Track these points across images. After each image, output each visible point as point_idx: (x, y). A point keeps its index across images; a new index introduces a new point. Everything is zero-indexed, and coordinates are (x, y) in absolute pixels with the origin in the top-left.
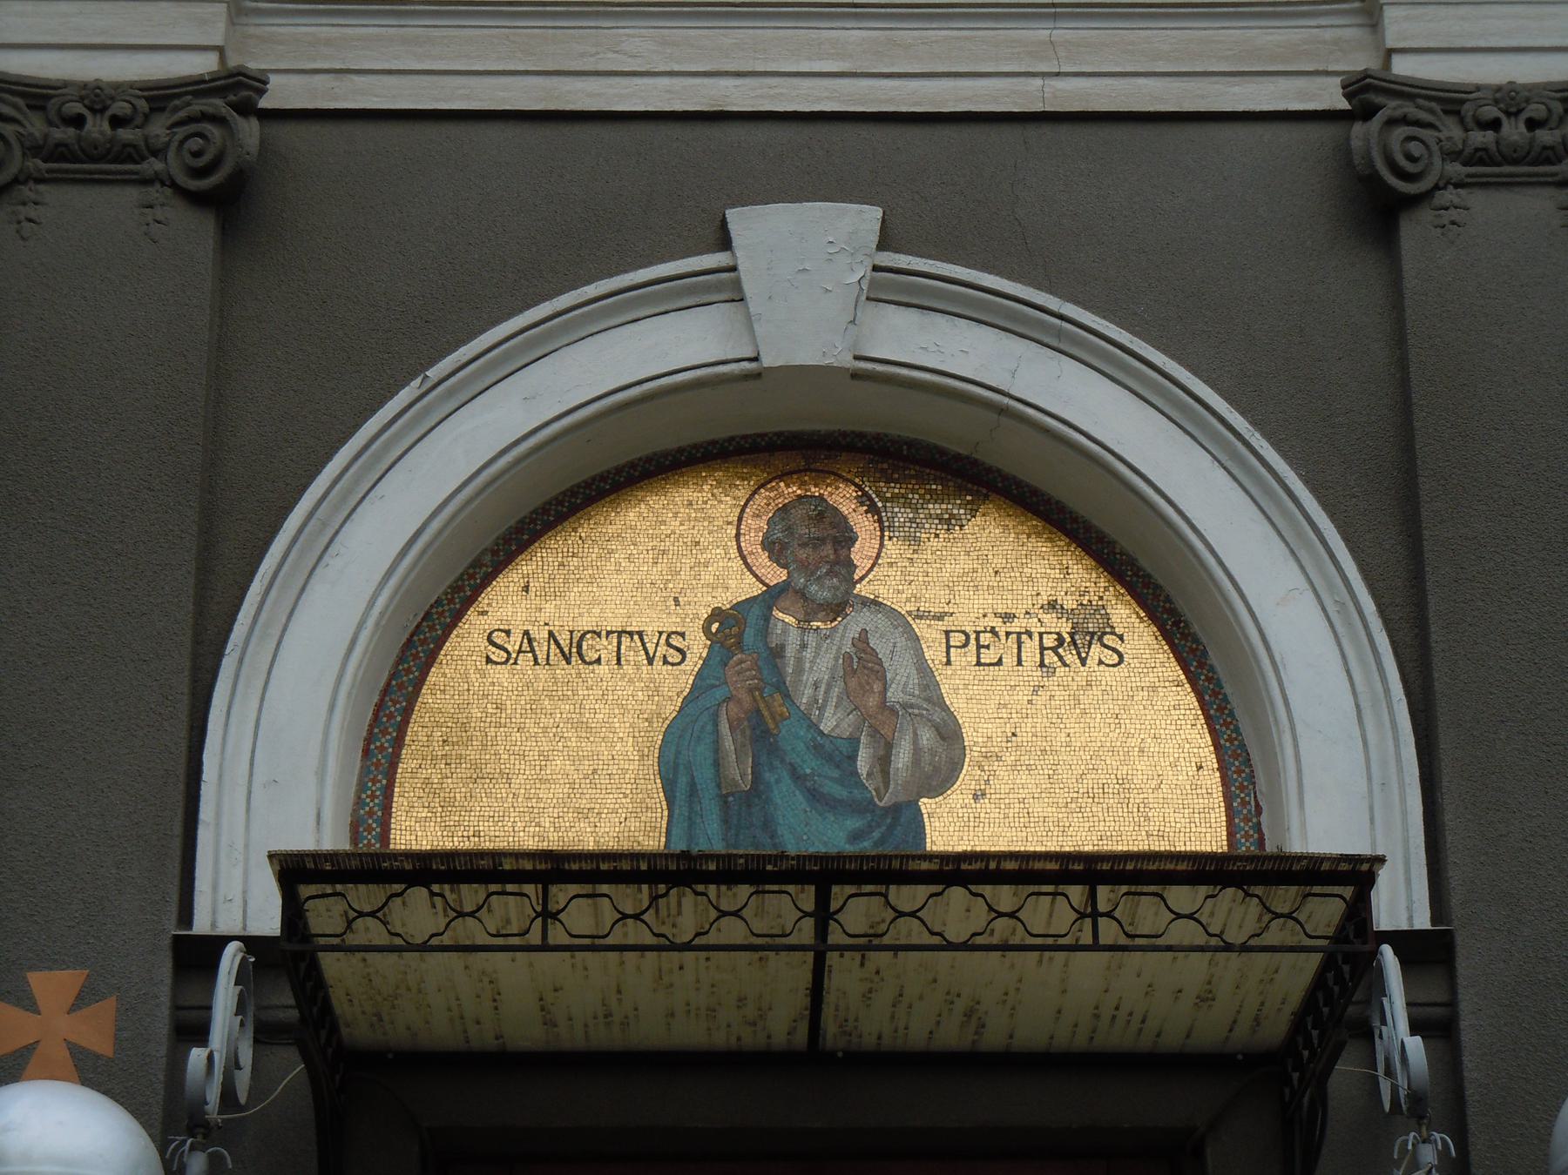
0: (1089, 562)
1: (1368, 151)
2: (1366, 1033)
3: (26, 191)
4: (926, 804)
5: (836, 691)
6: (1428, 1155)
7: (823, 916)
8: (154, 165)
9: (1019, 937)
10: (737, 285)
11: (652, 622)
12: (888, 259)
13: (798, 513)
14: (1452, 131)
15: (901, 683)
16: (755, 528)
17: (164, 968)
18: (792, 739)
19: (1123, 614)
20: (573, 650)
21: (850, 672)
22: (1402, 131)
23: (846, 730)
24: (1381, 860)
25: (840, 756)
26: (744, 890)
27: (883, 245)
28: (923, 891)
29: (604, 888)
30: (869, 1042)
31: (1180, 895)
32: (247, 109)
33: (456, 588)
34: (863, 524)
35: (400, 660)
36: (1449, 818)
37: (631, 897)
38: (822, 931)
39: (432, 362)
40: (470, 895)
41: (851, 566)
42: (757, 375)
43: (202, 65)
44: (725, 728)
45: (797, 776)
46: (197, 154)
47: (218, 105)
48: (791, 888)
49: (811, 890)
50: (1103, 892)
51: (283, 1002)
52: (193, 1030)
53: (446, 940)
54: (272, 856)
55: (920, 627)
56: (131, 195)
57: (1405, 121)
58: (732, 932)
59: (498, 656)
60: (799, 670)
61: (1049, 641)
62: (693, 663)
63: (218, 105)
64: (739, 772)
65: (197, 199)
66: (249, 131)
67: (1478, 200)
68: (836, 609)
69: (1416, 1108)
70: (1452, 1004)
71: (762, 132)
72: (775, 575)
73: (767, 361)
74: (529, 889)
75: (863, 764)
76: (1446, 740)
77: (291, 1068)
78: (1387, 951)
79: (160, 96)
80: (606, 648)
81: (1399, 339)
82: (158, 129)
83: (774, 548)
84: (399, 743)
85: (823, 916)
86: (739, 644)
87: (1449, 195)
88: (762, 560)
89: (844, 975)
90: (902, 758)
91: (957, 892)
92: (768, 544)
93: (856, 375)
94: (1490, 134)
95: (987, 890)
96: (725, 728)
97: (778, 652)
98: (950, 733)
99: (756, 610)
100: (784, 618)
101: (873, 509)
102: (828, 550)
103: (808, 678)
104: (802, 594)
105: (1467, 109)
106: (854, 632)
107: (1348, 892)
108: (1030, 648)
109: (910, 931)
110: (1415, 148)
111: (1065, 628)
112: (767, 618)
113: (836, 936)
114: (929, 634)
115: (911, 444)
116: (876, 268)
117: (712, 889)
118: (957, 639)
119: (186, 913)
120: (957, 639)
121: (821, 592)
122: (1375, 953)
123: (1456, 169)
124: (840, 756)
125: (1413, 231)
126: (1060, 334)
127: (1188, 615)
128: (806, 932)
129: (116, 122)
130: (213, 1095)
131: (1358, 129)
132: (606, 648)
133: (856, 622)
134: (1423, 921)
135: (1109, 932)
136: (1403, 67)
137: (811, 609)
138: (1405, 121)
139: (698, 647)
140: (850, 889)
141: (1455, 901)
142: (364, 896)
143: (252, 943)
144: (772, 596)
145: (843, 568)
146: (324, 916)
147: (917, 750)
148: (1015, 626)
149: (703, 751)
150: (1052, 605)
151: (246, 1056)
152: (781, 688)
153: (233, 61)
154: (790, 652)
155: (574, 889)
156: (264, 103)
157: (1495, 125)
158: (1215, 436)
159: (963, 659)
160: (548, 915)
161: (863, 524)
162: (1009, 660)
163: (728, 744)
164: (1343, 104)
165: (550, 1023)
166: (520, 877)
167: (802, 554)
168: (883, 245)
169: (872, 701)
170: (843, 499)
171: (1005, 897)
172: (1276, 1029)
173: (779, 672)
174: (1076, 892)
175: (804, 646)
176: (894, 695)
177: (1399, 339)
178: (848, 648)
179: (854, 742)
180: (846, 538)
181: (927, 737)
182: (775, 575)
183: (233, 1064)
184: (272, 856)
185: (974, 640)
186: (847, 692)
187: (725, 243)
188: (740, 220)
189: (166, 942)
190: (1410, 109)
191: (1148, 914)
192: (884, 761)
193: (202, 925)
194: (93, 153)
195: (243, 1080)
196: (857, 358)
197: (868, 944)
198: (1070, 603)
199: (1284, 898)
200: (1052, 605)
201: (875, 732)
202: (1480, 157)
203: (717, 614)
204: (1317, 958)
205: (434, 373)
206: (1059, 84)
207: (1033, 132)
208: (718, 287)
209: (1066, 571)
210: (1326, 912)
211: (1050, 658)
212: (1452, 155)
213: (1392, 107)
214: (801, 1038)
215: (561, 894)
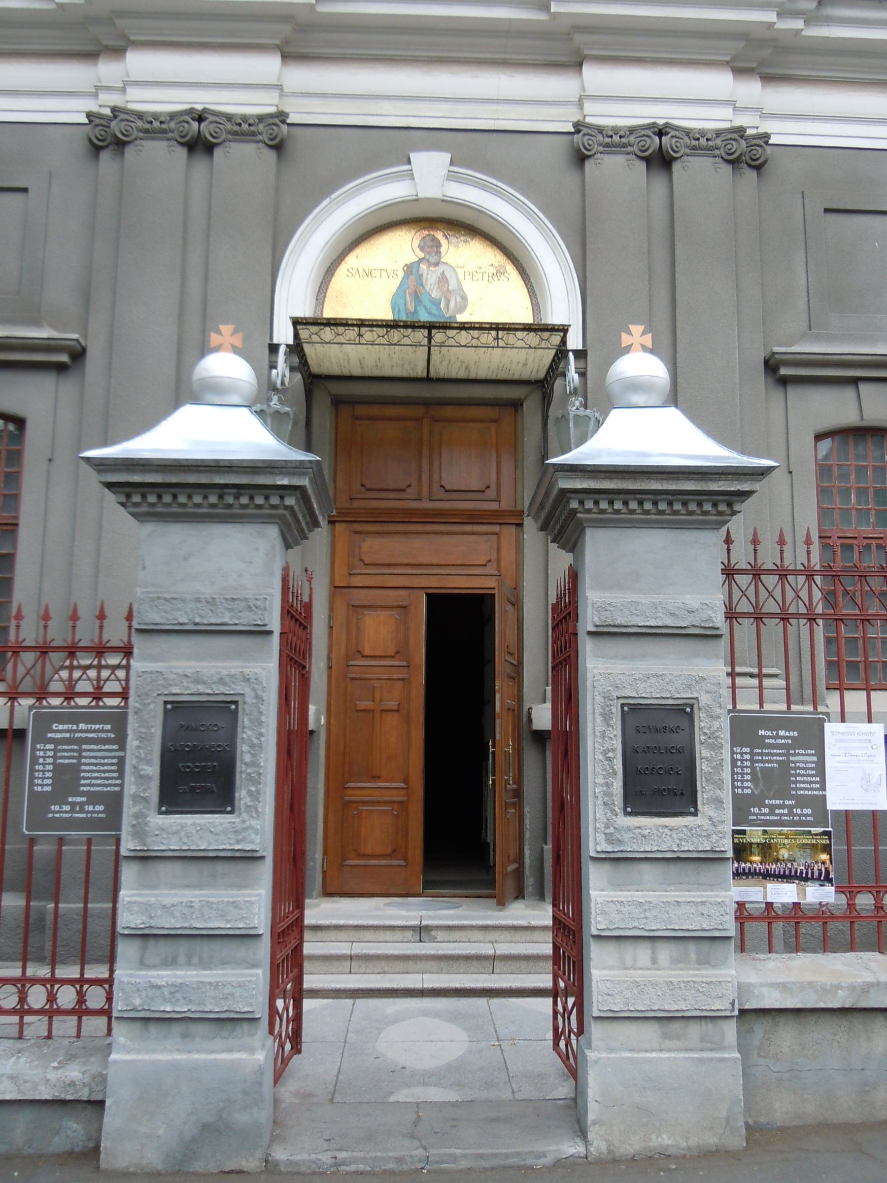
0: (502, 254)
1: (578, 142)
2: (564, 375)
3: (227, 144)
5: (436, 287)
6: (577, 403)
7: (430, 338)
8: (260, 137)
9: (480, 345)
10: (412, 175)
12: (453, 168)
13: (427, 239)
14: (600, 138)
15: (453, 285)
16: (417, 242)
17: (267, 351)
18: (425, 299)
19: (510, 268)
20: (369, 274)
21: (439, 281)
22: (587, 137)
23: (438, 297)
24: (570, 326)
25: (437, 304)
26: (410, 330)
28: (455, 332)
29: (375, 329)
30: (441, 376)
31: (520, 334)
32: (283, 122)
33: (339, 256)
34: (443, 241)
35: (326, 274)
36: (588, 321)
37: (382, 331)
38: (430, 342)
39: (332, 193)
40: (341, 329)
42: (417, 200)
43: (272, 110)
44: (408, 295)
45: (425, 307)
46: (271, 134)
47: (277, 121)
48: (422, 330)
49: (427, 331)
50: (500, 333)
51: (296, 361)
52: (273, 366)
53: (335, 341)
54: (290, 318)
55: (458, 270)
56: (254, 145)
57: (588, 134)
58: (406, 341)
59: (350, 275)
61: (491, 275)
62: (400, 278)
63: (277, 121)
65: (271, 147)
66: (285, 128)
67: (606, 157)
68: (437, 264)
69: (575, 392)
70: (586, 368)
71: (420, 133)
72: (422, 255)
73: (420, 196)
74: (356, 329)
75: (442, 306)
76: (589, 301)
77: (298, 376)
78: (571, 355)
79: (261, 118)
80: (377, 273)
81: (584, 194)
82: (261, 127)
83: (421, 248)
84: (325, 297)
85: (430, 338)
86: (412, 274)
87: (598, 155)
88: (418, 251)
89: (435, 357)
90: (452, 304)
91: (463, 332)
93: (443, 201)
94: (610, 139)
95: (471, 332)
96: (408, 295)
97: (422, 275)
98: (464, 298)
99: (415, 266)
100: (423, 267)
101: (446, 238)
102: (435, 249)
103: (429, 283)
104: (428, 261)
105: (604, 132)
106: (441, 271)
107: (562, 334)
108: (486, 276)
109: (452, 342)
110: (590, 142)
111: (495, 272)
112: (419, 267)
113: (433, 343)
114: (459, 271)
115: (457, 221)
116: (449, 171)
117: (402, 330)
118: (467, 274)
119: (271, 338)
120: (467, 274)
121: (433, 260)
122: (568, 354)
123: (601, 148)
124: (437, 304)
125: (589, 165)
126: (496, 191)
127: (526, 268)
128: (425, 341)
129: (250, 125)
130: (279, 383)
131: (576, 136)
132: (377, 273)
133: (441, 268)
134: (580, 347)
135: (501, 343)
136: (589, 120)
137: (430, 264)
138: (588, 134)
139: (401, 274)
140: (436, 331)
141: (588, 342)
142: (314, 329)
143: (288, 345)
144: (421, 260)
145: (439, 253)
146: (304, 333)
147: (456, 302)
148: (482, 271)
149: (402, 302)
150: (492, 265)
151: (287, 374)
152: (422, 285)
153: (280, 109)
154: (424, 276)
155: (367, 329)
156: (288, 121)
157: (611, 137)
158: (535, 219)
159: (469, 278)
160: (360, 335)
161: (443, 241)
163: (408, 299)
164: (573, 130)
165: (362, 368)
166: (353, 325)
167: (428, 250)
168: (451, 164)
169: (445, 289)
170: (439, 235)
171: (475, 333)
172: (541, 375)
173: (421, 281)
174: (494, 333)
175: (428, 274)
177: (584, 194)
178: (439, 275)
179: (440, 300)
180: (439, 245)
181: (459, 299)
182: (422, 255)
183: (284, 376)
184: (290, 318)
186: (439, 287)
187: (409, 162)
188: (414, 156)
189: (267, 345)
190: (590, 132)
191: (511, 338)
192: (448, 305)
193: (275, 341)
194: (243, 134)
195: (287, 380)
196: (444, 196)
197: (442, 345)
198: (496, 265)
199: (546, 335)
200: (492, 265)
201: (446, 297)
202: (607, 145)
204: (553, 352)
205: (333, 196)
206: (498, 122)
207: (491, 134)
208: (407, 175)
209: (495, 256)
210: (556, 339)
211: (490, 278)
212: (600, 144)
213: (585, 130)
214: (425, 375)
215: (363, 330)
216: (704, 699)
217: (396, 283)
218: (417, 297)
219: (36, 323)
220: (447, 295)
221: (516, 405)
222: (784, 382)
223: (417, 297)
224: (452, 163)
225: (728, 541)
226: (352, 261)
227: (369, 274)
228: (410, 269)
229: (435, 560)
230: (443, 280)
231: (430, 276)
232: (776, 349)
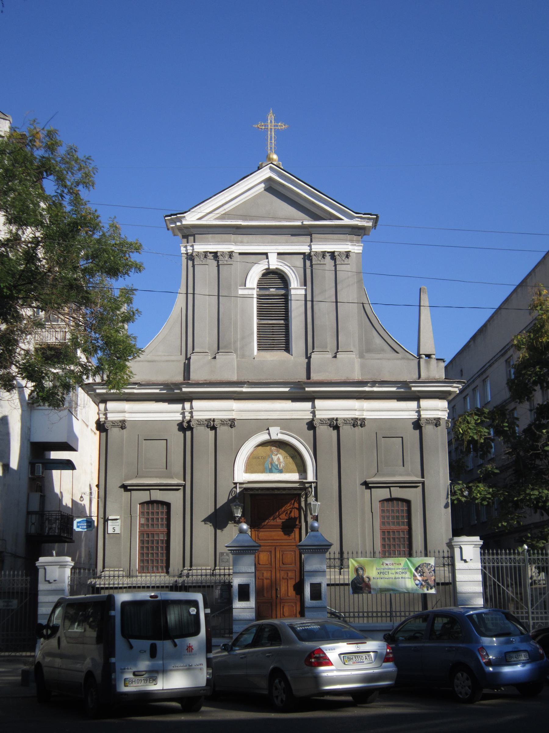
18: (274, 464)
25: (277, 466)
64: (270, 467)
68: (277, 454)
90: (281, 466)
124: (277, 466)
133: (279, 455)
187: (268, 429)
192: (280, 466)
216: (323, 582)
218: (271, 464)
219: (171, 478)
221: (299, 496)
222: (370, 488)
223: (271, 464)
224: (280, 429)
225: (330, 553)
227: (258, 458)
229: (278, 538)
230: (279, 459)
231: (275, 458)
232: (367, 480)
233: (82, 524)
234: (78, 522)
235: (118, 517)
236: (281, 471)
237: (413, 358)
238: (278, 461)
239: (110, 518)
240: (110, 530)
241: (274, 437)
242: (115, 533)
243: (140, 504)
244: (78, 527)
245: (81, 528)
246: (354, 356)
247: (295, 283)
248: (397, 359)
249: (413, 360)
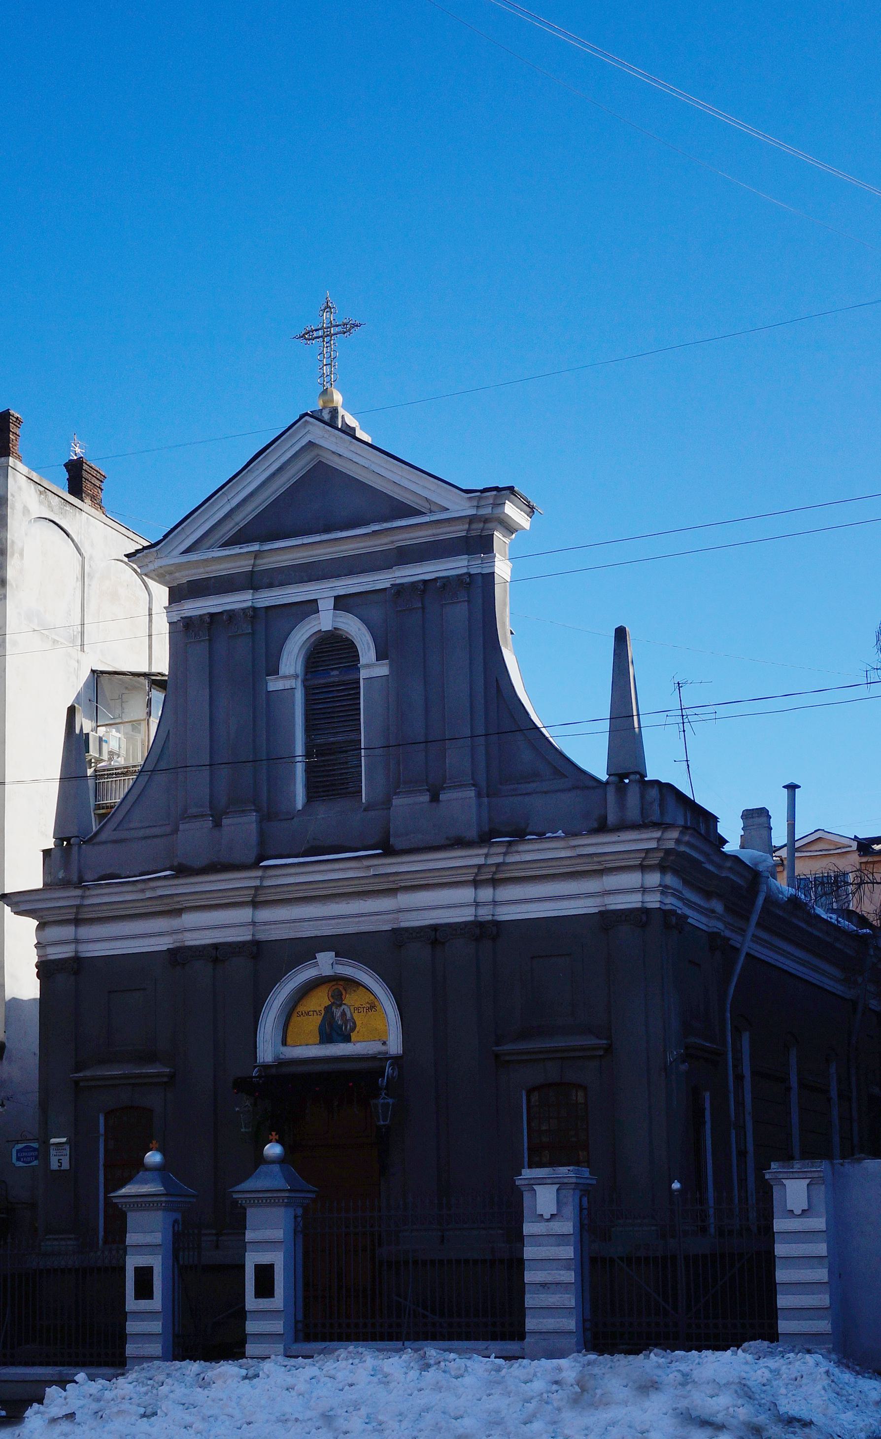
4: (351, 1034)
11: (318, 1009)
12: (337, 958)
15: (349, 1016)
20: (308, 1014)
27: (336, 957)
34: (344, 993)
41: (342, 999)
60: (336, 1015)
62: (323, 1014)
64: (328, 1030)
68: (340, 1005)
72: (332, 1001)
90: (348, 1027)
92: (332, 996)
98: (354, 1023)
100: (334, 1009)
103: (337, 1016)
104: (336, 1003)
108: (365, 1009)
114: (352, 1008)
118: (356, 1009)
133: (343, 1007)
139: (323, 1012)
144: (333, 1004)
147: (350, 1027)
148: (363, 1006)
154: (335, 1012)
162: (362, 1011)
168: (336, 957)
169: (344, 1019)
176: (348, 1018)
180: (342, 994)
182: (332, 1001)
185: (358, 1009)
187: (316, 959)
192: (346, 1027)
203: (325, 1007)
217: (320, 1018)
220: (346, 1022)
226: (301, 1008)
228: (328, 1009)
230: (344, 1014)
231: (338, 1013)
233: (25, 1154)
234: (18, 1151)
235: (64, 1140)
236: (347, 1039)
237: (595, 784)
238: (342, 1019)
239: (53, 1141)
240: (54, 1165)
241: (327, 971)
242: (62, 1168)
243: (107, 1115)
244: (18, 1159)
245: (24, 1162)
246: (472, 794)
247: (367, 652)
248: (562, 791)
249: (594, 788)
